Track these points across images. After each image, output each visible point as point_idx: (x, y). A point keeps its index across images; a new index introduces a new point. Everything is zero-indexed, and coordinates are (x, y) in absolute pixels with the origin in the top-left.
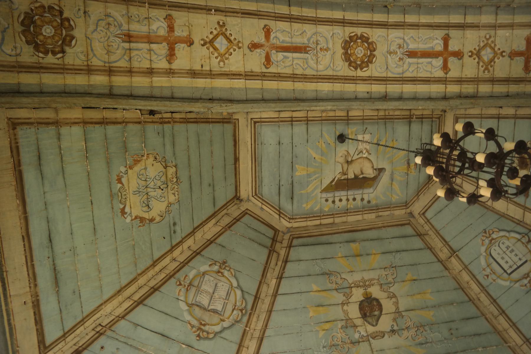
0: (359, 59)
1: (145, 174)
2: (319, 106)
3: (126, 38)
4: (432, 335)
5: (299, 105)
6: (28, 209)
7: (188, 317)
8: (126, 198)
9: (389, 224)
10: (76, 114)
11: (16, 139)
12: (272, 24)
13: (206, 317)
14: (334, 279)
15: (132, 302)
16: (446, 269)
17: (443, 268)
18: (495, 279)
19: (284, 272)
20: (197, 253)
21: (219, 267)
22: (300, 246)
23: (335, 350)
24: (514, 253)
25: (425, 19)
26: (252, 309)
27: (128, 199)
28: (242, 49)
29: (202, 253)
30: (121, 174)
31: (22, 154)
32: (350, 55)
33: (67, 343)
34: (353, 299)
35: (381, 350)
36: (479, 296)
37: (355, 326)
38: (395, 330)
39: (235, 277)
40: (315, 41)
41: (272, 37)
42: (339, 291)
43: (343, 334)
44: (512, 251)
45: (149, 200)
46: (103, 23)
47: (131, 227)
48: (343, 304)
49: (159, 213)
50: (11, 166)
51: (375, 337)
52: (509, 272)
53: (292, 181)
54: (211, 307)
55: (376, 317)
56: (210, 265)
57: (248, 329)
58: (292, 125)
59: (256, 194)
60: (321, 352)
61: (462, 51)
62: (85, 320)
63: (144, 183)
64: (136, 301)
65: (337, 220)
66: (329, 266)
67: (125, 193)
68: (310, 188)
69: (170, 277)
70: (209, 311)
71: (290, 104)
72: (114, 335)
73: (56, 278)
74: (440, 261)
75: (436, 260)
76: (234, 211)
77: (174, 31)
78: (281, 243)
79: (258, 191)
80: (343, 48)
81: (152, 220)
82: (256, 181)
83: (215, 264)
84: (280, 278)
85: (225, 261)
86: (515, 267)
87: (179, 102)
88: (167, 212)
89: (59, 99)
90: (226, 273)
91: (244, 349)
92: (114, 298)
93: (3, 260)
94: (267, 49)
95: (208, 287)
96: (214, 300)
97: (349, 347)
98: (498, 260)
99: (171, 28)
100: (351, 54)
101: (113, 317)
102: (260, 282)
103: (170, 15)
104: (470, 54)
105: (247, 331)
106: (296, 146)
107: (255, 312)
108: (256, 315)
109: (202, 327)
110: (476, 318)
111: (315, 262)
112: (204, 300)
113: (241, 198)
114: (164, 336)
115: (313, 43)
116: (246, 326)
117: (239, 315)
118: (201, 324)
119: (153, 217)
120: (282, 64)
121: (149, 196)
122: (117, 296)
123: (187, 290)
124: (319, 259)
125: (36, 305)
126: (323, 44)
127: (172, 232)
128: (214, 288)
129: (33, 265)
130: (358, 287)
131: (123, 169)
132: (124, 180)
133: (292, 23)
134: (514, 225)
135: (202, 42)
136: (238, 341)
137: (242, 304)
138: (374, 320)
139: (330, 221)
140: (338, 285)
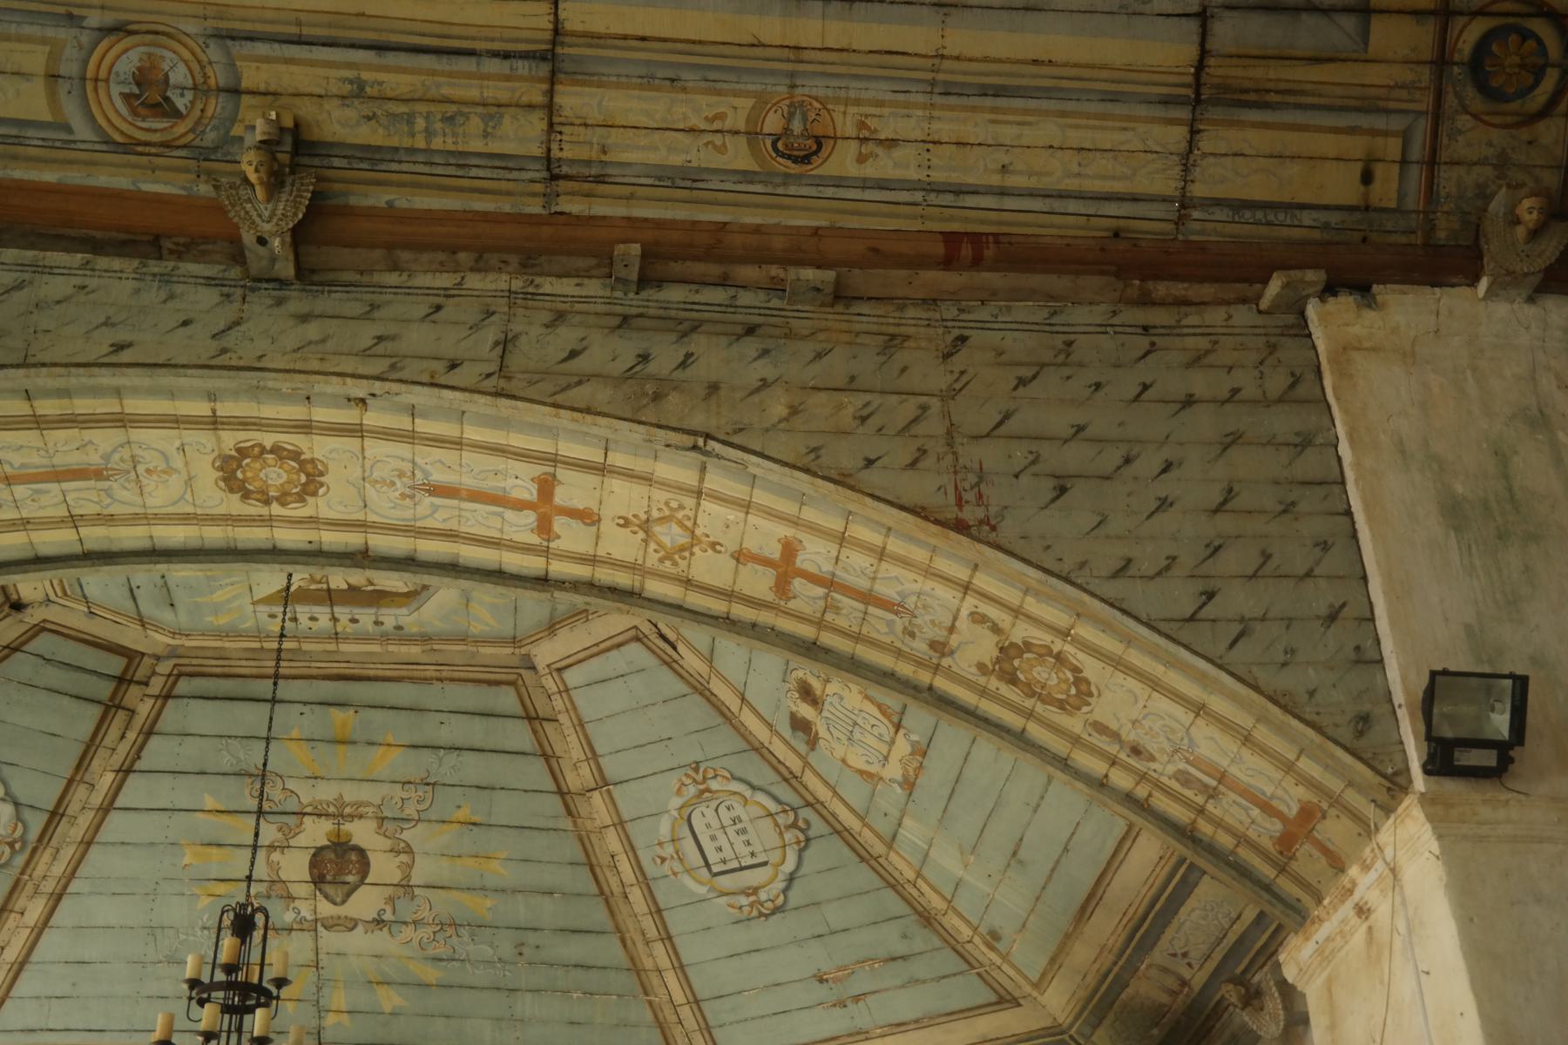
4: (471, 947)
9: (456, 675)
16: (570, 813)
17: (562, 810)
18: (676, 870)
22: (194, 697)
24: (744, 838)
26: (40, 840)
32: (244, 481)
34: (301, 840)
36: (628, 890)
37: (291, 898)
44: (744, 831)
51: (332, 927)
52: (715, 869)
57: (26, 877)
59: (65, 594)
61: (596, 511)
74: (561, 793)
75: (553, 787)
78: (146, 684)
80: (221, 469)
84: (125, 771)
86: (735, 865)
98: (700, 837)
102: (70, 782)
104: (622, 522)
105: (22, 884)
108: (49, 851)
110: (598, 933)
115: (122, 460)
116: (22, 873)
130: (320, 815)
133: (45, 432)
134: (774, 777)
137: (14, 832)
140: (272, 804)
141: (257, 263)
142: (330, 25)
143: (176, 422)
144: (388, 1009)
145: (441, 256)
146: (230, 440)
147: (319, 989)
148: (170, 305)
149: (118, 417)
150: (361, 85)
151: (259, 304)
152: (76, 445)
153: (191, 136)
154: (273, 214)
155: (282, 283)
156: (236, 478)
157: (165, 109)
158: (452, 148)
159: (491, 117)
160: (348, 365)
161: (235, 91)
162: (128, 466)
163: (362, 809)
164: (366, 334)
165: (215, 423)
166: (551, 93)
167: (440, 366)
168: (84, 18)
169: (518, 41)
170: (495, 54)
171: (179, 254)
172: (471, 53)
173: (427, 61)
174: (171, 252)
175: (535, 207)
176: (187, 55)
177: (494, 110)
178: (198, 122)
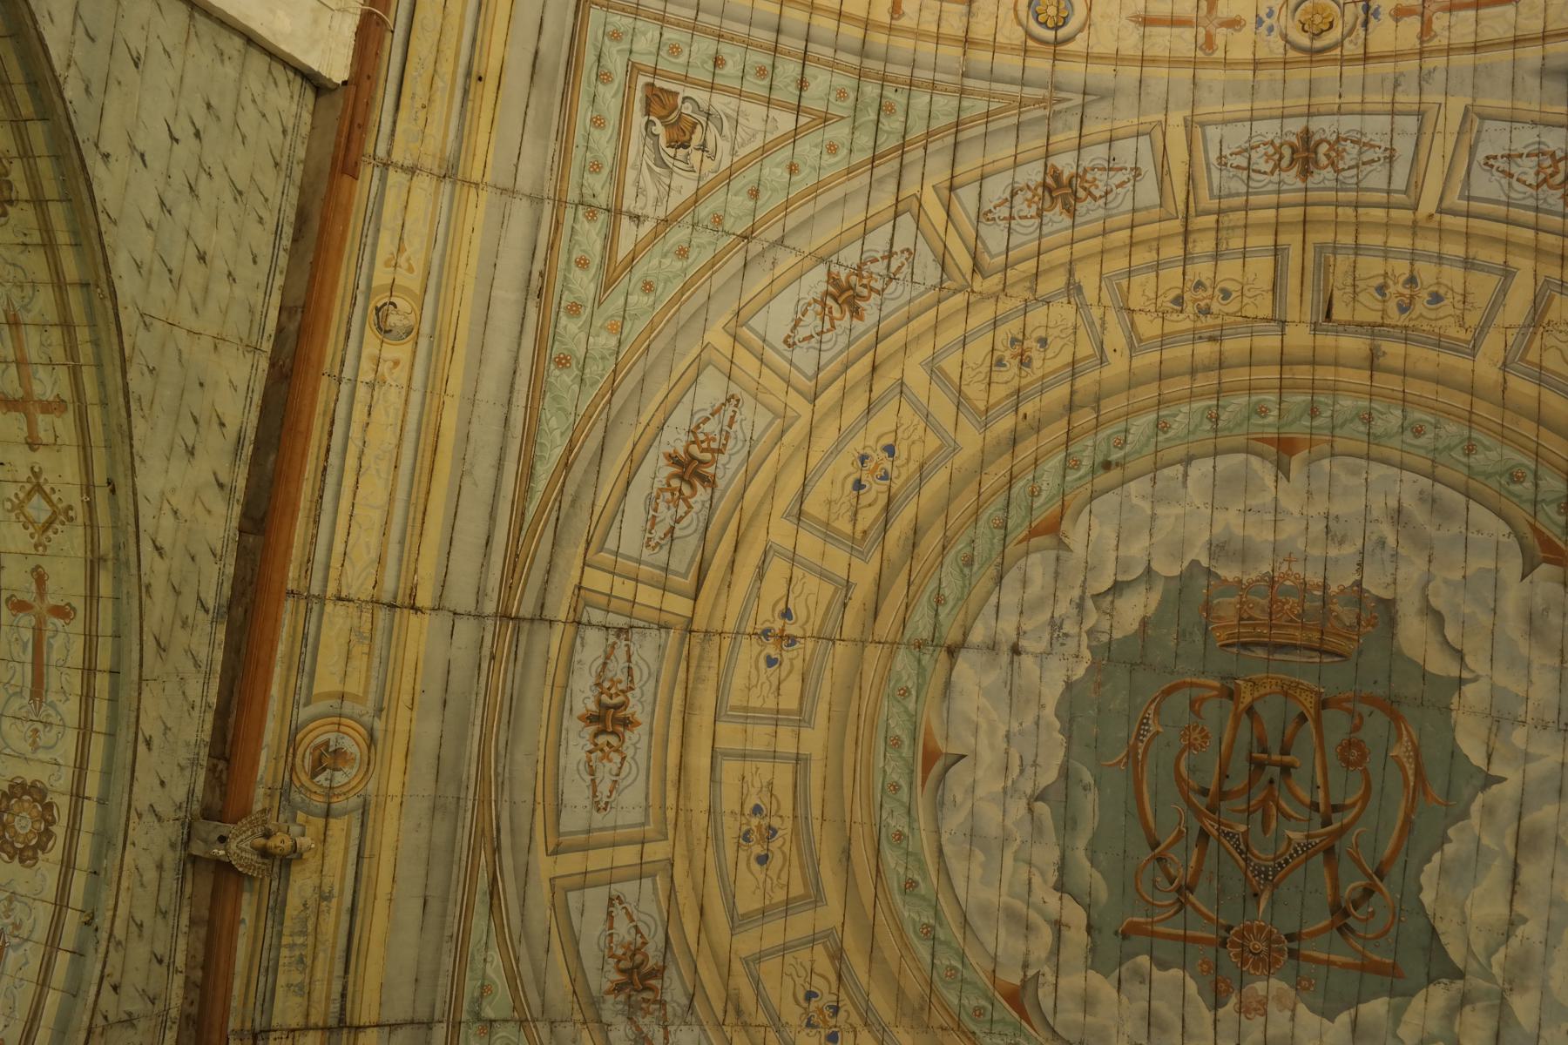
0: (10, 819)
3: (11, 319)
12: (78, 625)
25: (52, 1000)
28: (33, 552)
32: (20, 798)
40: (50, 720)
41: (55, 620)
46: (20, 276)
77: (43, 412)
80: (33, 786)
94: (37, 605)
99: (46, 407)
100: (23, 801)
103: (66, 409)
115: (48, 715)
120: (15, 636)
126: (47, 737)
135: (36, 470)
141: (203, 827)
142: (369, 877)
143: (81, 767)
145: (200, 958)
146: (62, 803)
148: (177, 769)
149: (89, 726)
150: (328, 898)
151: (172, 831)
152: (65, 688)
153: (298, 784)
154: (243, 850)
155: (186, 844)
156: (23, 794)
157: (318, 768)
158: (281, 963)
159: (301, 989)
160: (122, 911)
161: (328, 814)
162: (43, 717)
164: (144, 915)
165: (78, 795)
166: (316, 1028)
167: (115, 979)
168: (380, 718)
169: (353, 1002)
170: (345, 988)
171: (212, 770)
172: (346, 971)
173: (342, 941)
174: (215, 766)
175: (233, 1023)
176: (353, 783)
177: (305, 991)
178: (307, 789)
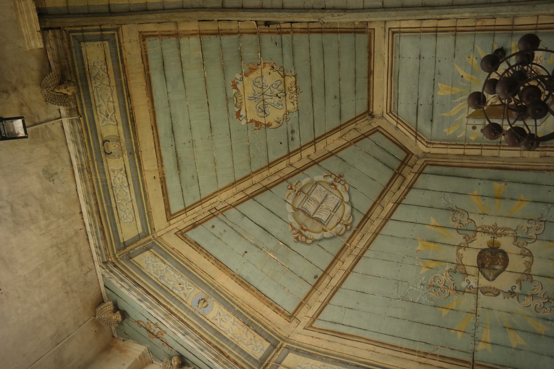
1: (261, 82)
2: (453, 14)
5: (427, 13)
6: (155, 105)
7: (291, 219)
8: (241, 103)
10: (193, 26)
11: (145, 49)
13: (309, 223)
14: (459, 218)
15: (244, 195)
19: (404, 198)
20: (315, 163)
21: (333, 179)
23: (433, 291)
26: (358, 227)
27: (244, 104)
29: (320, 164)
30: (236, 81)
31: (150, 61)
33: (187, 216)
34: (474, 244)
35: (488, 309)
37: (466, 274)
38: (514, 293)
39: (348, 192)
42: (460, 231)
43: (449, 278)
45: (265, 106)
47: (246, 129)
48: (460, 246)
49: (276, 119)
50: (142, 70)
51: (486, 293)
53: (433, 101)
54: (315, 216)
55: (495, 272)
56: (325, 176)
57: (348, 245)
58: (436, 36)
59: (391, 112)
60: (417, 288)
62: (203, 202)
63: (259, 90)
64: (247, 195)
65: (486, 153)
66: (459, 202)
67: (240, 98)
68: (454, 111)
69: (283, 180)
70: (313, 218)
71: (416, 12)
72: (224, 219)
73: (178, 163)
76: (364, 126)
78: (412, 167)
79: (393, 108)
81: (268, 125)
82: (391, 98)
83: (331, 176)
84: (398, 203)
85: (342, 175)
87: (288, 12)
88: (285, 120)
89: (177, 15)
90: (339, 187)
91: (339, 262)
92: (229, 188)
93: (138, 143)
95: (317, 196)
96: (321, 209)
97: (451, 293)
101: (226, 204)
102: (375, 203)
105: (346, 247)
106: (440, 61)
107: (360, 230)
109: (303, 232)
111: (443, 194)
112: (311, 208)
113: (374, 114)
114: (265, 230)
116: (347, 242)
117: (342, 229)
118: (302, 228)
119: (269, 122)
121: (266, 102)
122: (231, 187)
123: (297, 195)
124: (448, 192)
125: (163, 181)
127: (290, 139)
128: (323, 198)
129: (160, 150)
130: (485, 233)
131: (238, 76)
132: (239, 86)
136: (335, 253)
137: (349, 220)
138: (492, 273)
139: (477, 152)
140: (461, 225)
144: (514, 345)
147: (476, 327)
163: (506, 231)
